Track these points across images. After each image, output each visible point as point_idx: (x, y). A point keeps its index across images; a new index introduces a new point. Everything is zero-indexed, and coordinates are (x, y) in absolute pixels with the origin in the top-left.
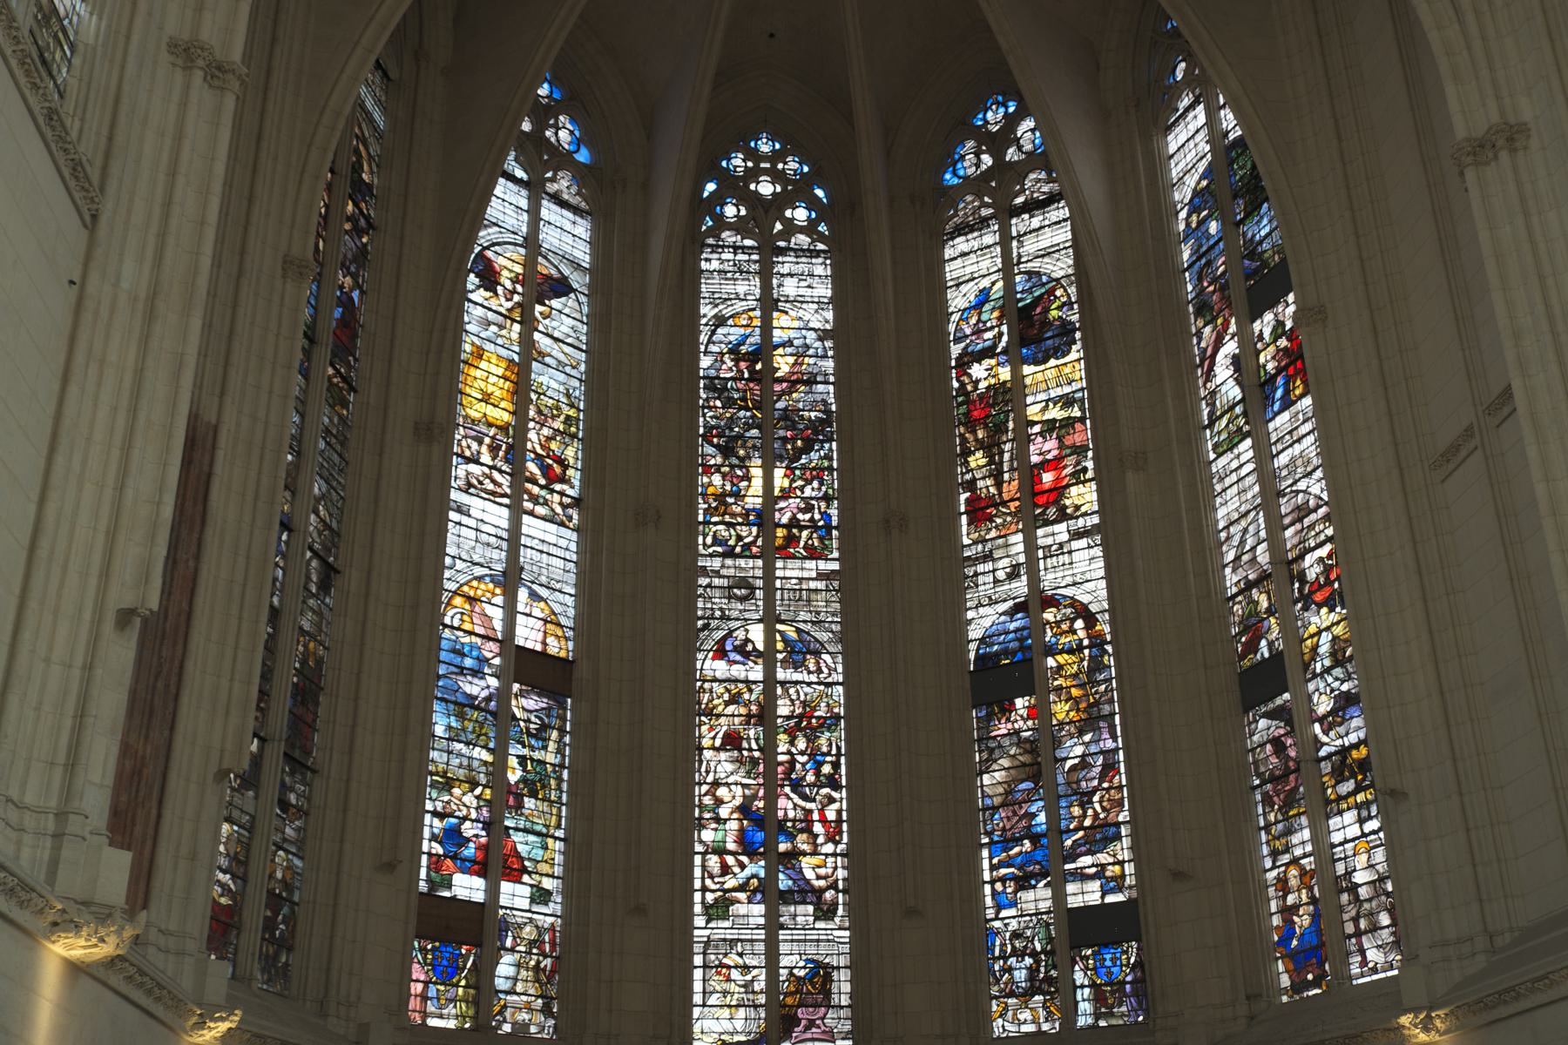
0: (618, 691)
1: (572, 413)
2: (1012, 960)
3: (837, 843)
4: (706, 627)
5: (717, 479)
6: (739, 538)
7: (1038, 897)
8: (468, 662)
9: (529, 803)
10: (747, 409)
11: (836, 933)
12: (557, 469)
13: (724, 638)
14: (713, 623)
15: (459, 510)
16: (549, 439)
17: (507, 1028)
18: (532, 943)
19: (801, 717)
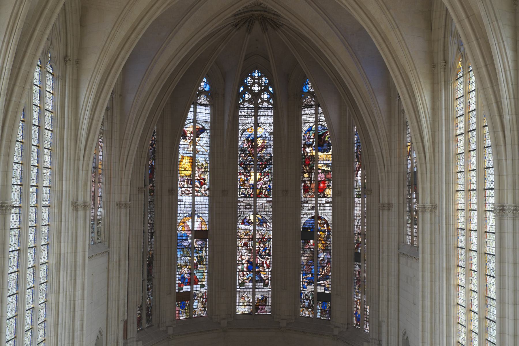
0: (220, 235)
1: (206, 165)
2: (305, 300)
3: (269, 269)
4: (240, 216)
5: (243, 176)
6: (248, 192)
7: (311, 288)
8: (184, 238)
9: (199, 266)
10: (250, 156)
12: (203, 182)
13: (244, 219)
14: (242, 215)
15: (180, 201)
17: (196, 316)
18: (201, 297)
19: (262, 239)
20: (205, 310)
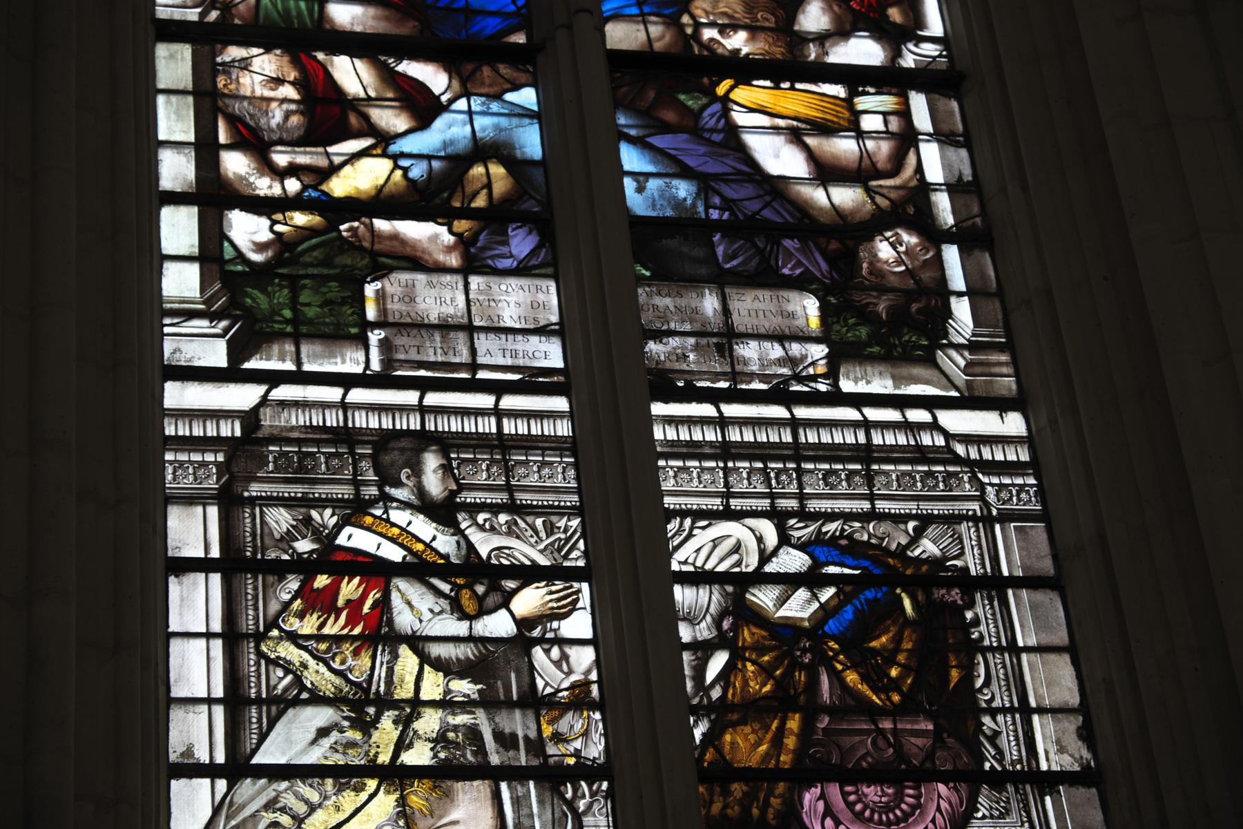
11: (955, 421)
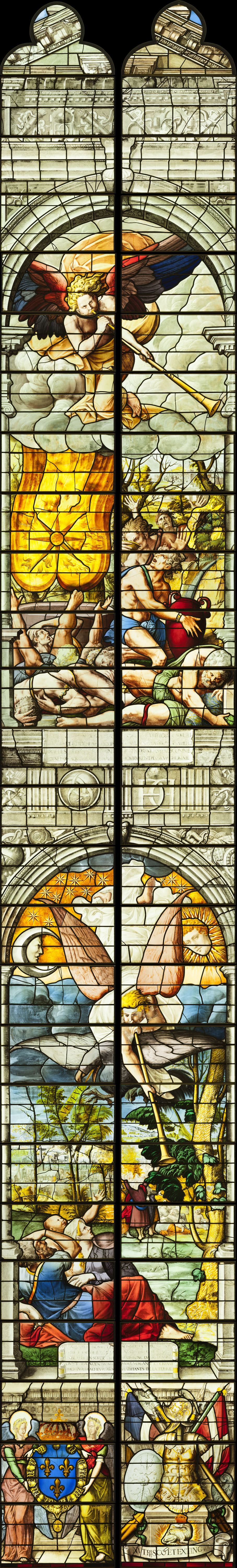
1: (212, 505)
12: (189, 624)
16: (167, 573)
20: (215, 1521)
